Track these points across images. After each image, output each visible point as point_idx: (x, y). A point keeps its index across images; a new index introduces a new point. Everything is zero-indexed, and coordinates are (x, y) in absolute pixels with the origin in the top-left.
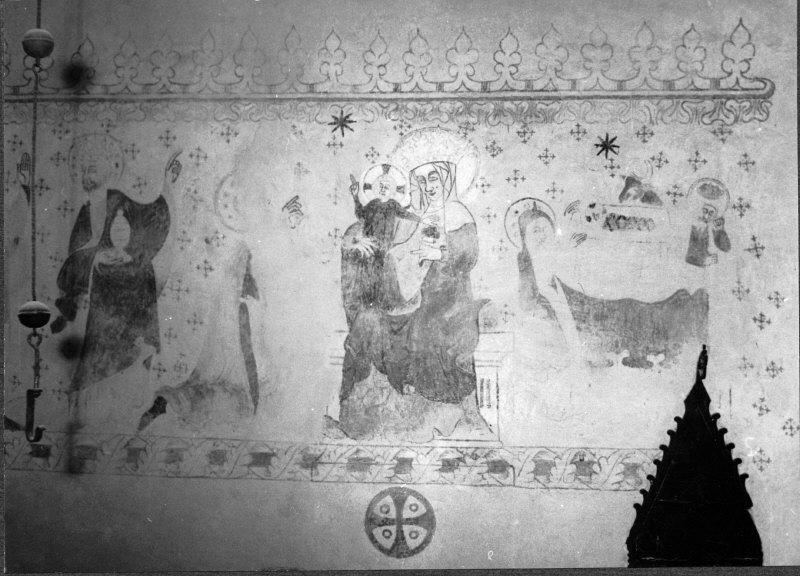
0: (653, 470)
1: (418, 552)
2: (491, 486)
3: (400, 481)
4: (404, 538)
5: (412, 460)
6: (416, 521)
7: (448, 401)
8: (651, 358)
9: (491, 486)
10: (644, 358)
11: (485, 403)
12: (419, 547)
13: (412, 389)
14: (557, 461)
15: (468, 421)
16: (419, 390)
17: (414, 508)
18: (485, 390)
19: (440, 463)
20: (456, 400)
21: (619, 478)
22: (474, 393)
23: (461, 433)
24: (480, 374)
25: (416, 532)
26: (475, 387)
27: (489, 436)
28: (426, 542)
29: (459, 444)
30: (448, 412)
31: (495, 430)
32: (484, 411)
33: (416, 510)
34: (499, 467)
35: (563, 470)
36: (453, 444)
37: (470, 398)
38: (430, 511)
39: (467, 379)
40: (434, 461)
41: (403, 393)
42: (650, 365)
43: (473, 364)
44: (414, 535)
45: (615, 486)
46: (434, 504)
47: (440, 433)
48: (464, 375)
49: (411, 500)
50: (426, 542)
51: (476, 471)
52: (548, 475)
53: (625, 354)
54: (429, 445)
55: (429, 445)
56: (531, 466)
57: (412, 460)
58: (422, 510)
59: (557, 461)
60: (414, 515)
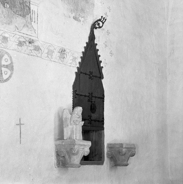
0: (80, 60)
1: (7, 81)
2: (34, 56)
3: (3, 47)
4: (2, 74)
5: (8, 38)
6: (7, 67)
7: (21, 15)
8: (80, 18)
9: (34, 56)
10: (79, 18)
11: (33, 20)
12: (7, 79)
13: (8, 6)
14: (54, 50)
15: (27, 26)
16: (10, 7)
17: (6, 60)
18: (34, 15)
19: (18, 42)
20: (24, 16)
21: (71, 62)
22: (30, 14)
23: (25, 30)
24: (32, 7)
25: (7, 72)
26: (30, 12)
27: (34, 34)
28: (10, 77)
29: (25, 36)
30: (19, 21)
31: (37, 33)
32: (33, 23)
33: (7, 61)
34: (37, 49)
35: (56, 54)
36: (22, 35)
37: (29, 16)
38: (12, 63)
39: (27, 8)
40: (16, 41)
41: (4, 7)
42: (80, 21)
43: (30, 2)
44: (6, 73)
45: (70, 65)
46: (13, 59)
47: (18, 29)
48: (26, 6)
49: (6, 56)
50: (10, 77)
51: (29, 48)
52: (52, 56)
53: (74, 15)
54: (14, 33)
55: (14, 33)
56: (46, 51)
57: (8, 38)
58: (9, 62)
59: (54, 50)
60: (6, 64)
